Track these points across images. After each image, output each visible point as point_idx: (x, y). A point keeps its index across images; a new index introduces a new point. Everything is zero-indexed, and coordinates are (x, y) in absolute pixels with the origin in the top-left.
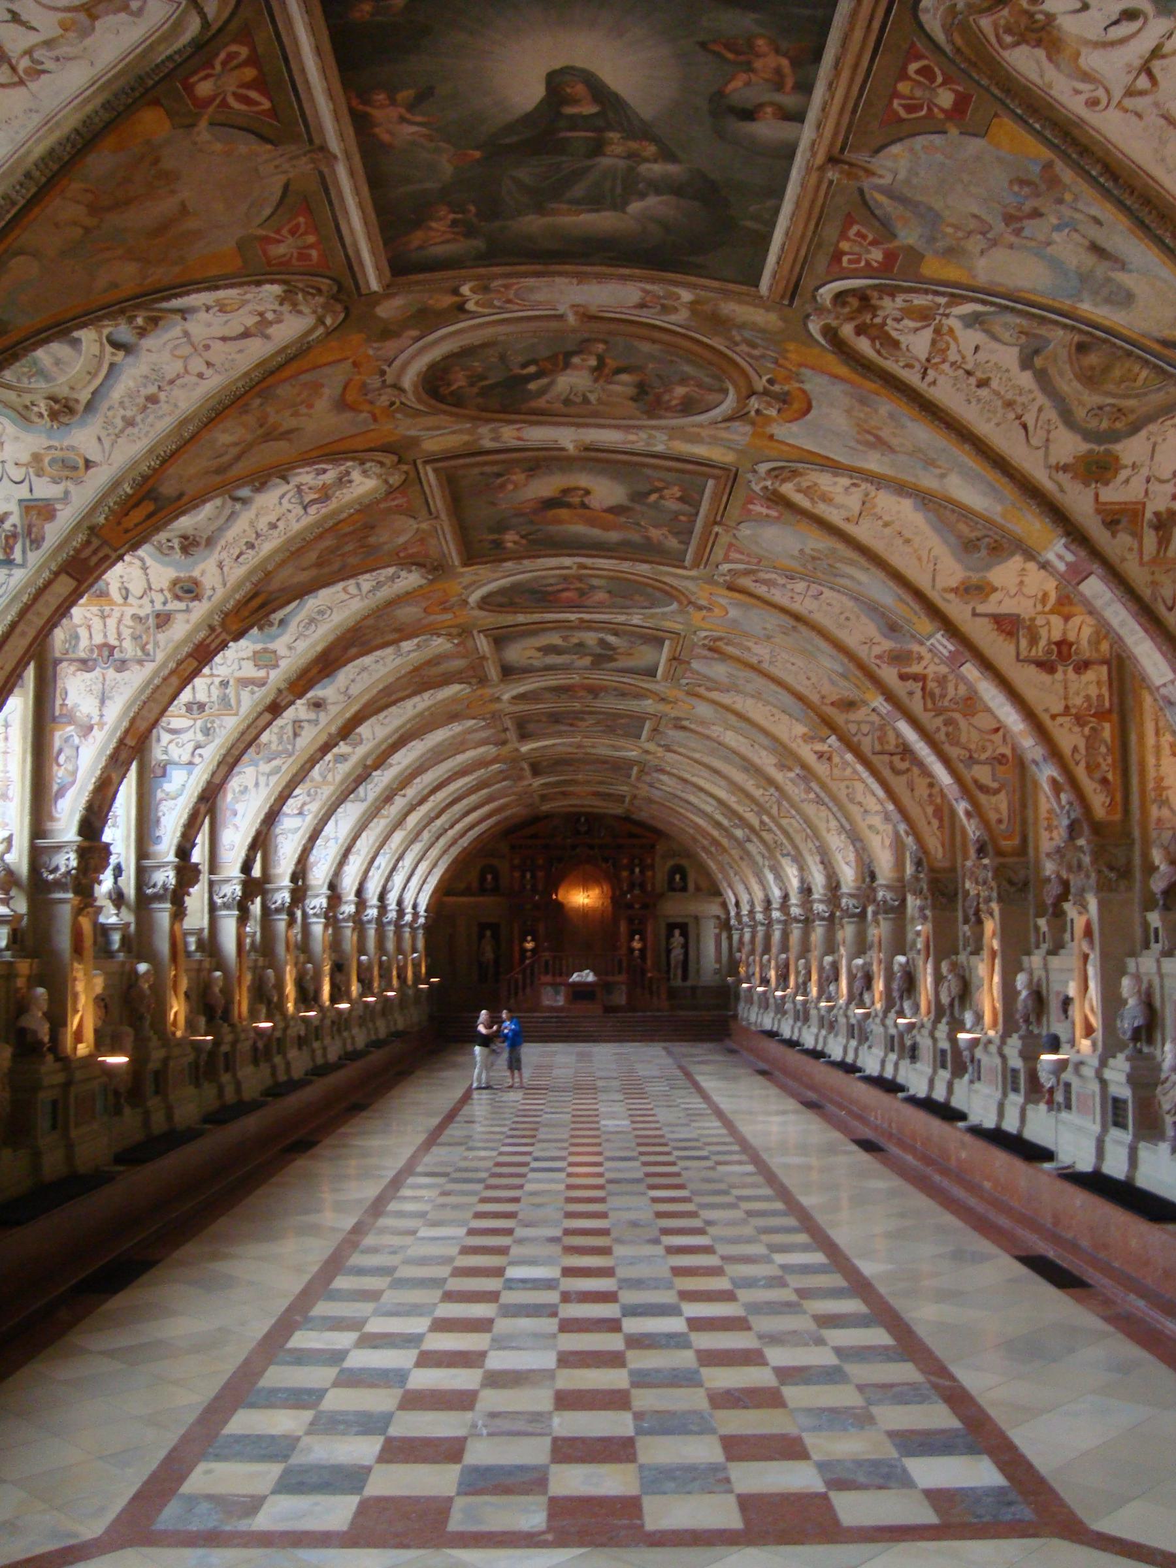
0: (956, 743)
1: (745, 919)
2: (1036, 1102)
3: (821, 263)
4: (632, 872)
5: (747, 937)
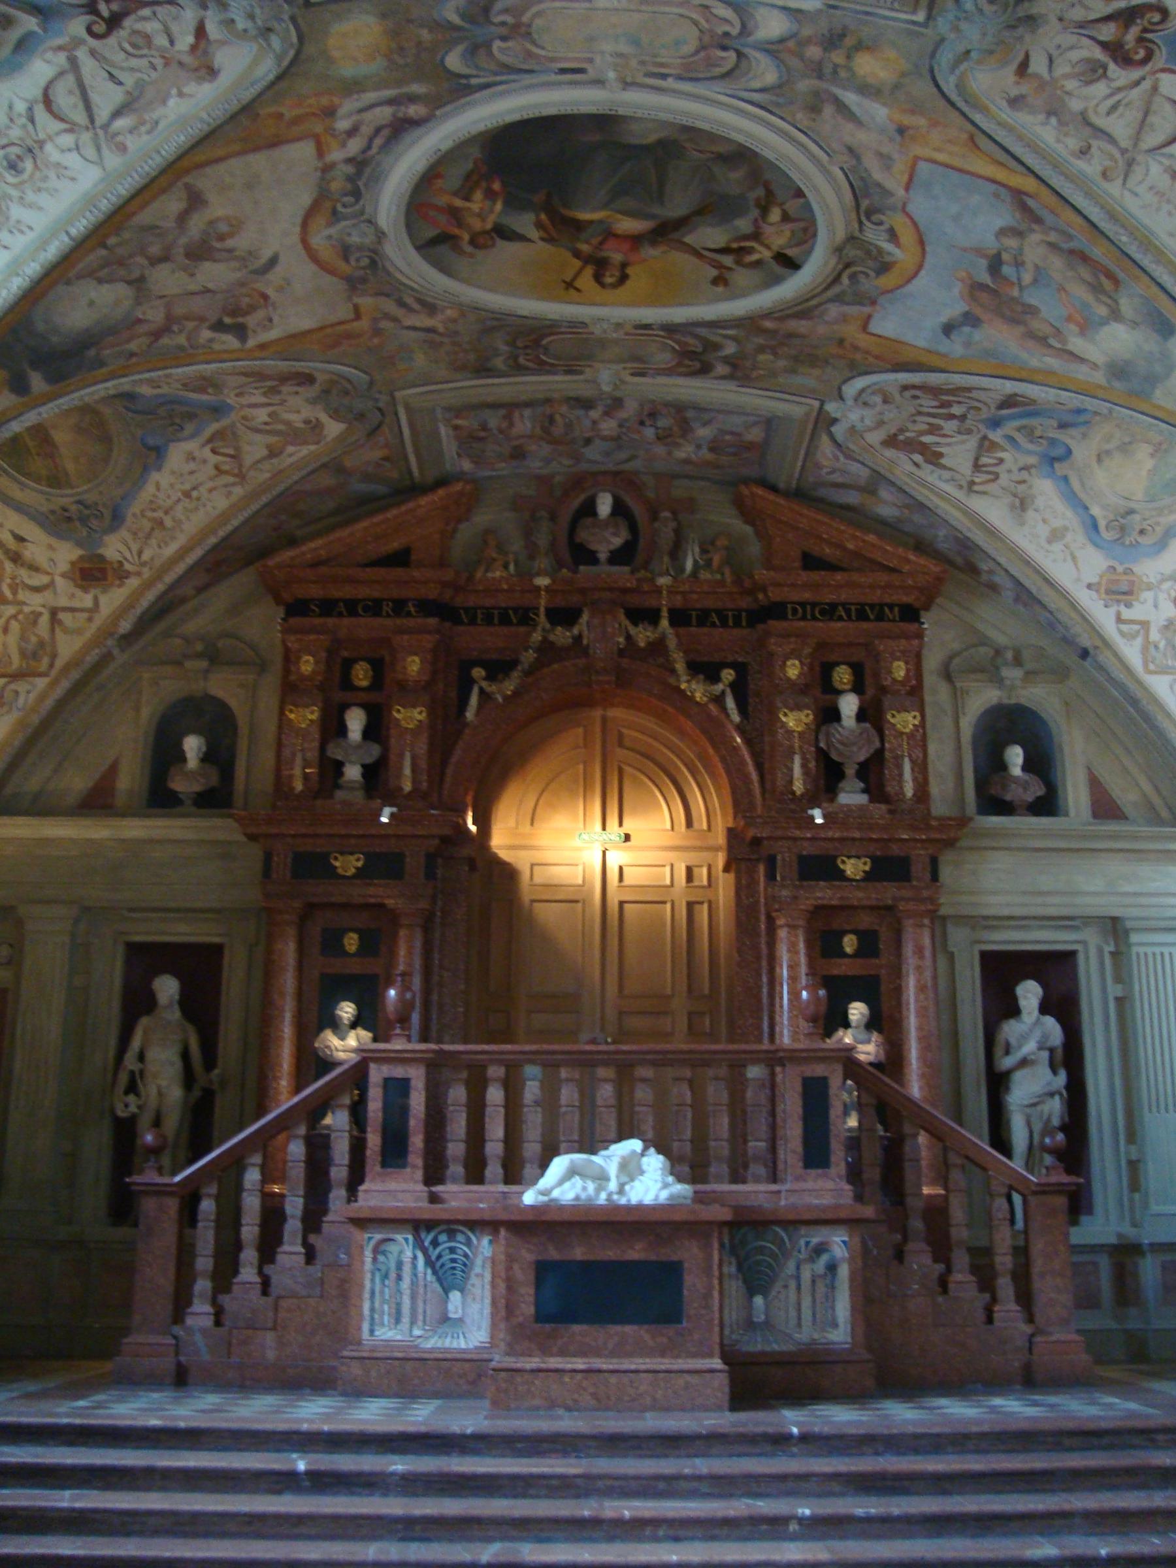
4: (831, 715)
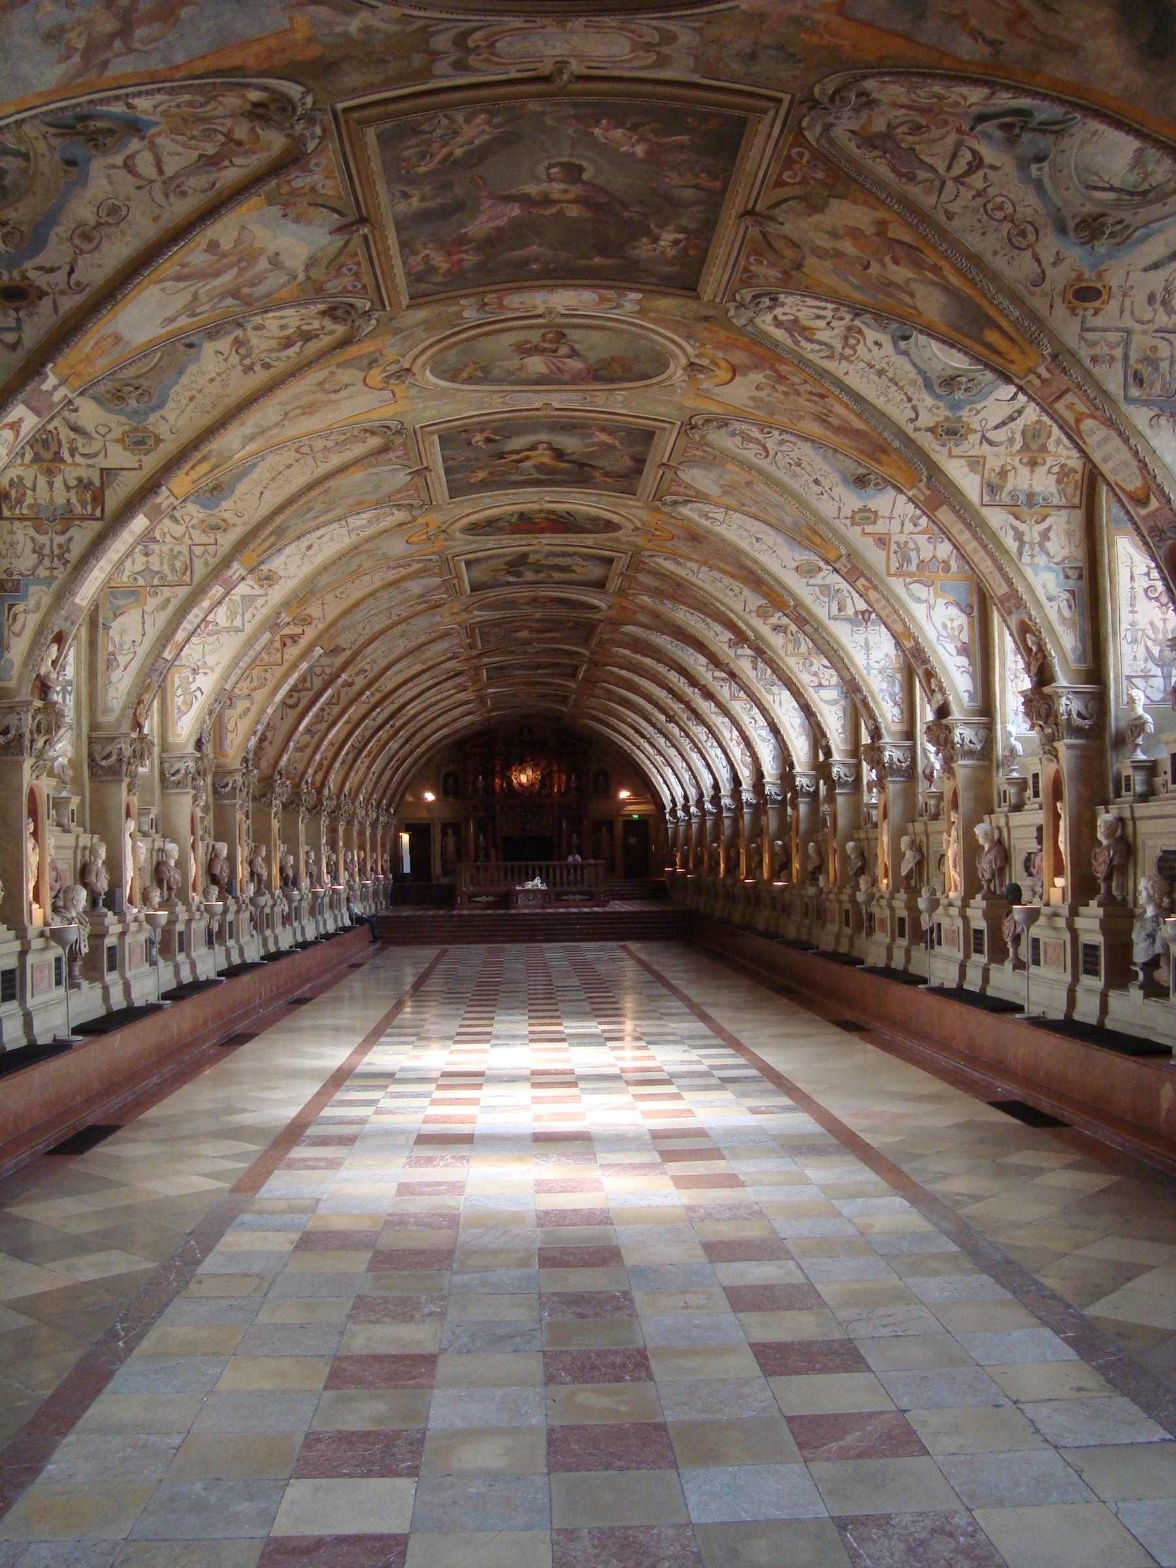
2: (1001, 961)
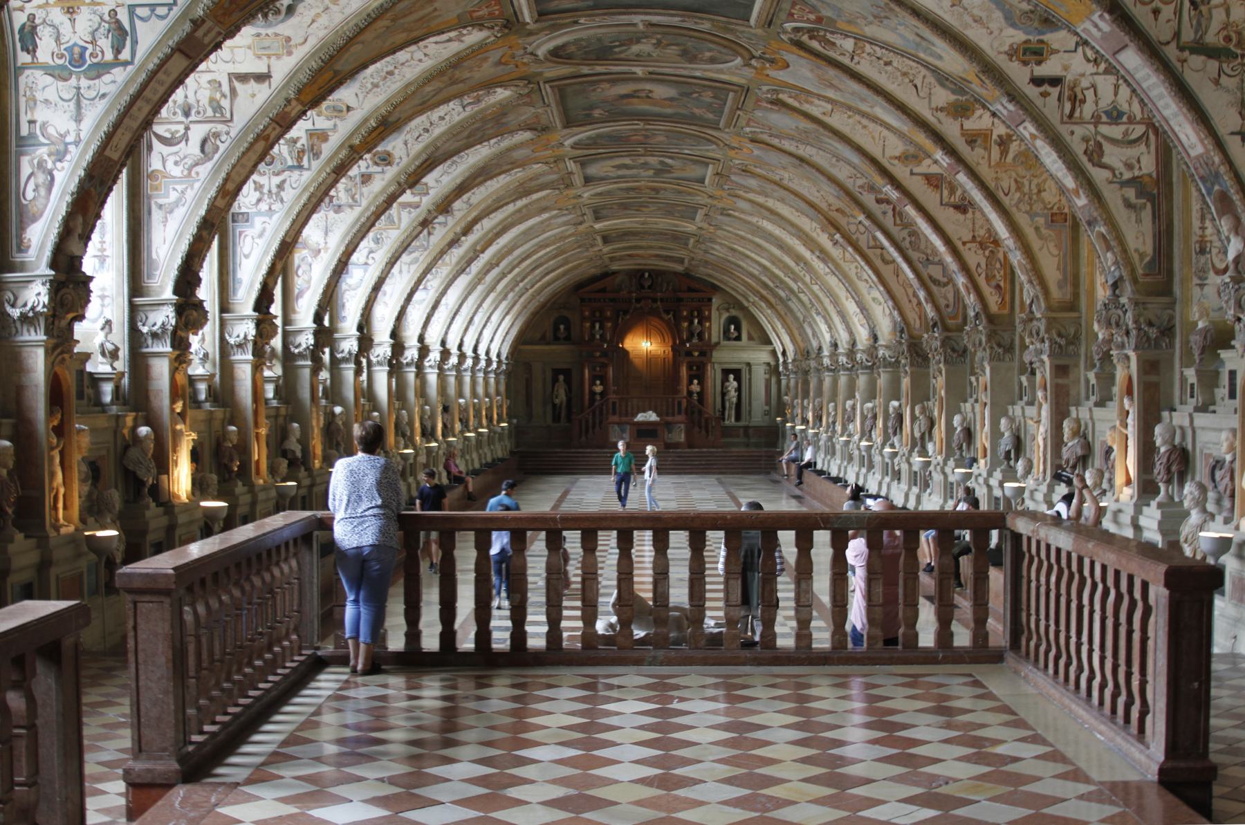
0: (917, 249)
1: (790, 366)
3: (783, 16)
4: (691, 323)
5: (792, 382)
